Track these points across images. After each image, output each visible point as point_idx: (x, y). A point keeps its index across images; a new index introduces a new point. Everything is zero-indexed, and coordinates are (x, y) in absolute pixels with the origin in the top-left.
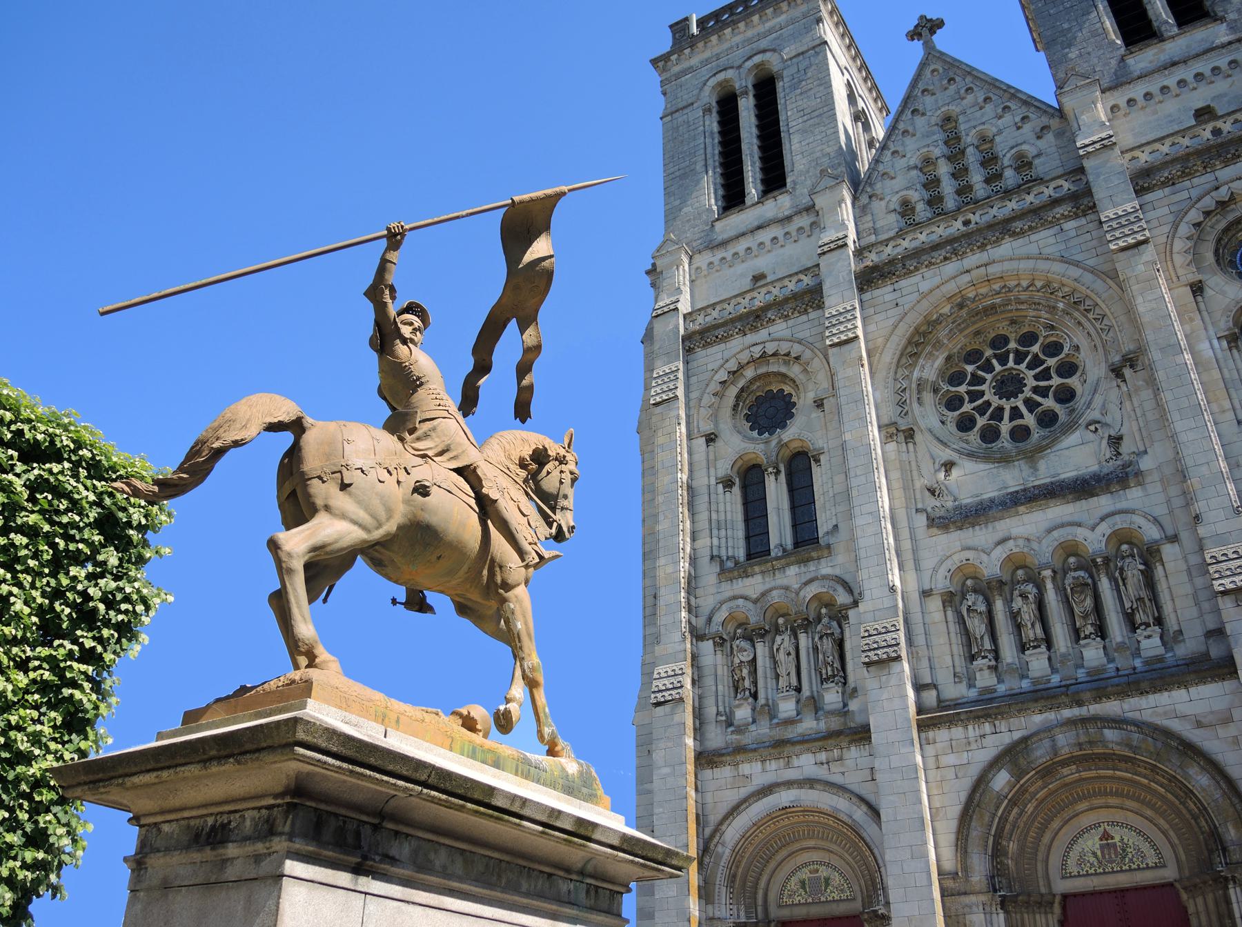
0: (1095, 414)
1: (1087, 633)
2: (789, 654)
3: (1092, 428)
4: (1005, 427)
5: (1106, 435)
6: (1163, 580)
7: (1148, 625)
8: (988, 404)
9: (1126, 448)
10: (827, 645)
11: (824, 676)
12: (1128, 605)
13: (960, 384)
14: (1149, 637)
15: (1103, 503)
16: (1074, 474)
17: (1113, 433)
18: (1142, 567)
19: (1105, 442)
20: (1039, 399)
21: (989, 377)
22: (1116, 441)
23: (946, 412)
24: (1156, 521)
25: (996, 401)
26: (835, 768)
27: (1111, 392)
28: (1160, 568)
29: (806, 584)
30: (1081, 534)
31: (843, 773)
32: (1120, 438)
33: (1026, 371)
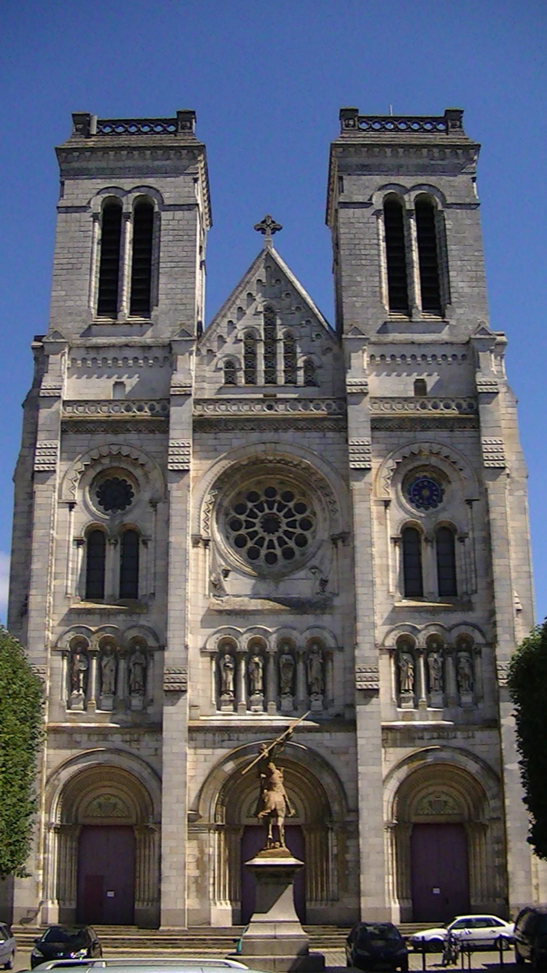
0: (315, 562)
1: (286, 691)
2: (112, 671)
3: (313, 571)
4: (263, 552)
5: (320, 578)
6: (330, 670)
7: (318, 694)
8: (256, 533)
9: (329, 588)
10: (138, 670)
11: (133, 688)
12: (310, 680)
13: (241, 514)
14: (316, 700)
15: (309, 619)
16: (297, 596)
17: (324, 578)
18: (321, 661)
19: (318, 582)
20: (286, 539)
21: (260, 514)
22: (324, 582)
23: (230, 530)
24: (335, 637)
25: (262, 533)
26: (134, 745)
27: (327, 551)
28: (330, 664)
29: (129, 628)
30: (295, 635)
31: (138, 749)
32: (326, 581)
33: (283, 518)
